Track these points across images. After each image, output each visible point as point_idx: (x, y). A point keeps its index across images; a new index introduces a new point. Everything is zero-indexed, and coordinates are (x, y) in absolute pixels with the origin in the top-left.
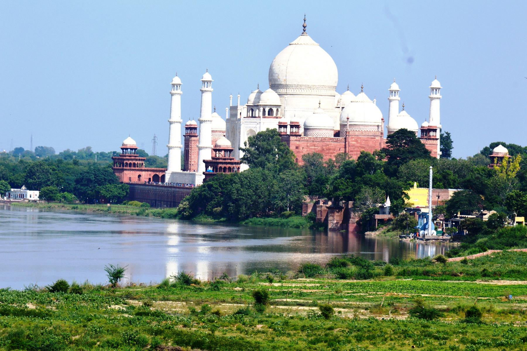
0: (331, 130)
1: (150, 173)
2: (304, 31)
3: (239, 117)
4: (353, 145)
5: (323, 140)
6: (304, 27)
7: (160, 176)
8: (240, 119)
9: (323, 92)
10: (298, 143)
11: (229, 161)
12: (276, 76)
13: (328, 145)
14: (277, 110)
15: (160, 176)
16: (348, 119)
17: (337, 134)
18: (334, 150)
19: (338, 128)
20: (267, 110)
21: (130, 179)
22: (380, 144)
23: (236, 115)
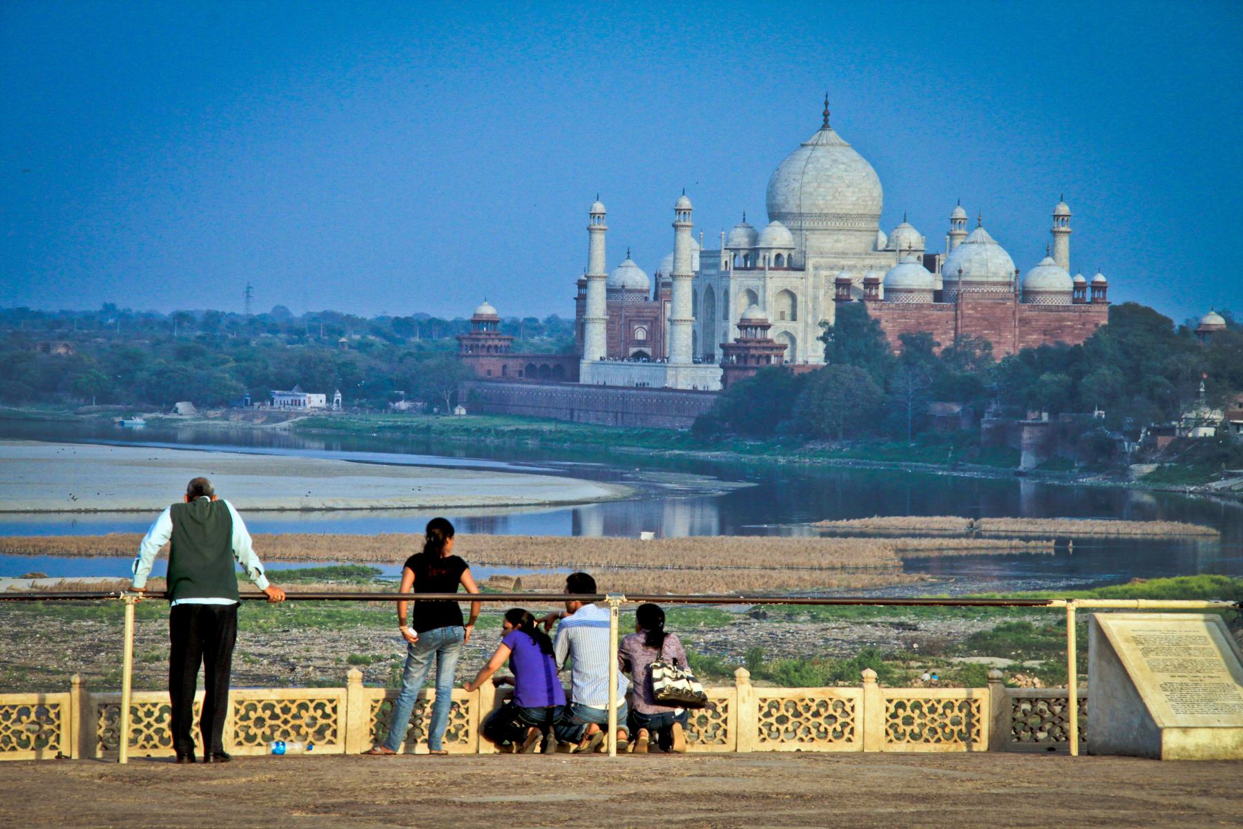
0: (930, 291)
1: (521, 361)
2: (826, 121)
3: (723, 269)
4: (970, 316)
5: (920, 307)
6: (826, 114)
7: (538, 366)
8: (727, 273)
9: (863, 225)
10: (877, 313)
11: (765, 345)
12: (780, 199)
13: (927, 316)
14: (790, 255)
15: (538, 366)
16: (960, 271)
17: (938, 296)
18: (937, 324)
19: (940, 287)
20: (773, 254)
21: (489, 372)
22: (1014, 313)
23: (717, 266)
